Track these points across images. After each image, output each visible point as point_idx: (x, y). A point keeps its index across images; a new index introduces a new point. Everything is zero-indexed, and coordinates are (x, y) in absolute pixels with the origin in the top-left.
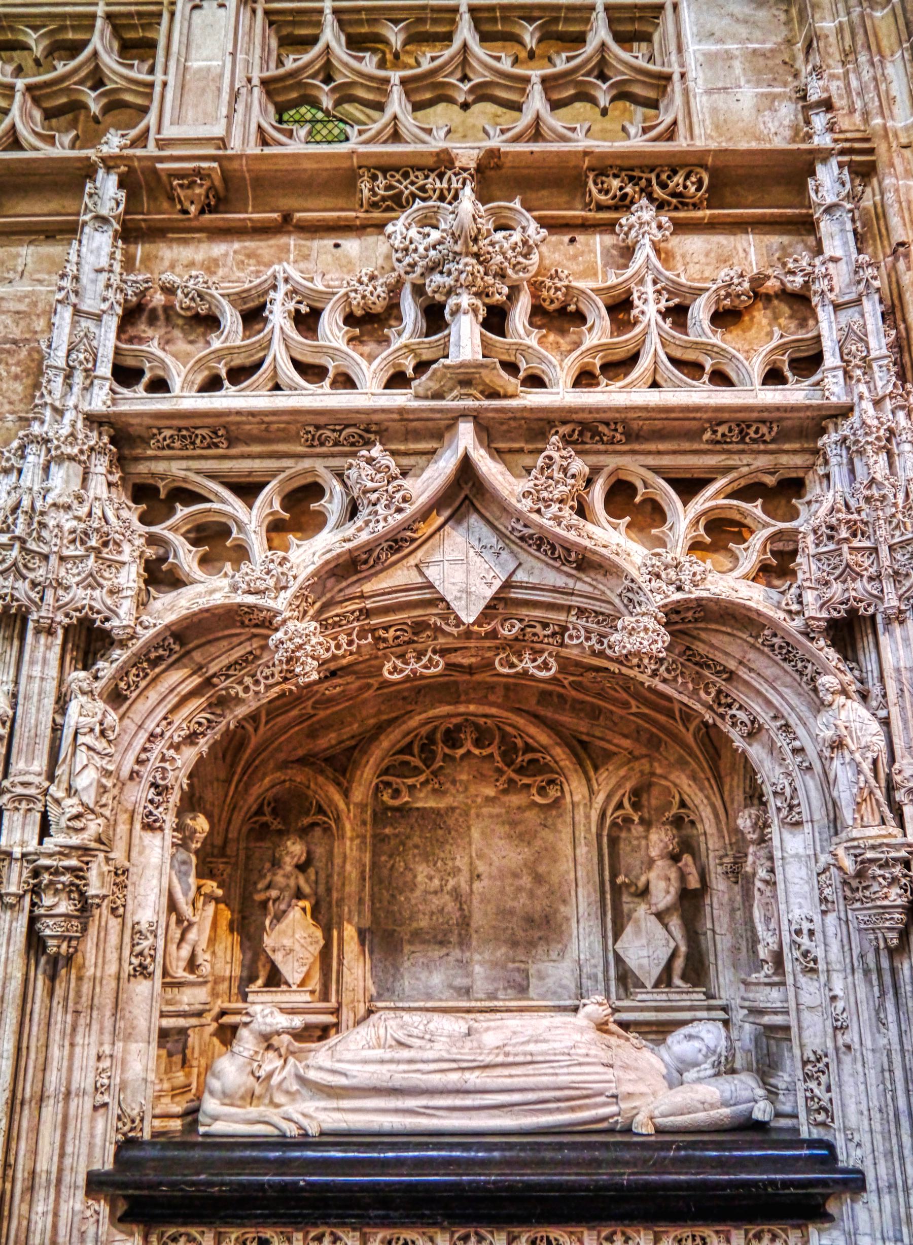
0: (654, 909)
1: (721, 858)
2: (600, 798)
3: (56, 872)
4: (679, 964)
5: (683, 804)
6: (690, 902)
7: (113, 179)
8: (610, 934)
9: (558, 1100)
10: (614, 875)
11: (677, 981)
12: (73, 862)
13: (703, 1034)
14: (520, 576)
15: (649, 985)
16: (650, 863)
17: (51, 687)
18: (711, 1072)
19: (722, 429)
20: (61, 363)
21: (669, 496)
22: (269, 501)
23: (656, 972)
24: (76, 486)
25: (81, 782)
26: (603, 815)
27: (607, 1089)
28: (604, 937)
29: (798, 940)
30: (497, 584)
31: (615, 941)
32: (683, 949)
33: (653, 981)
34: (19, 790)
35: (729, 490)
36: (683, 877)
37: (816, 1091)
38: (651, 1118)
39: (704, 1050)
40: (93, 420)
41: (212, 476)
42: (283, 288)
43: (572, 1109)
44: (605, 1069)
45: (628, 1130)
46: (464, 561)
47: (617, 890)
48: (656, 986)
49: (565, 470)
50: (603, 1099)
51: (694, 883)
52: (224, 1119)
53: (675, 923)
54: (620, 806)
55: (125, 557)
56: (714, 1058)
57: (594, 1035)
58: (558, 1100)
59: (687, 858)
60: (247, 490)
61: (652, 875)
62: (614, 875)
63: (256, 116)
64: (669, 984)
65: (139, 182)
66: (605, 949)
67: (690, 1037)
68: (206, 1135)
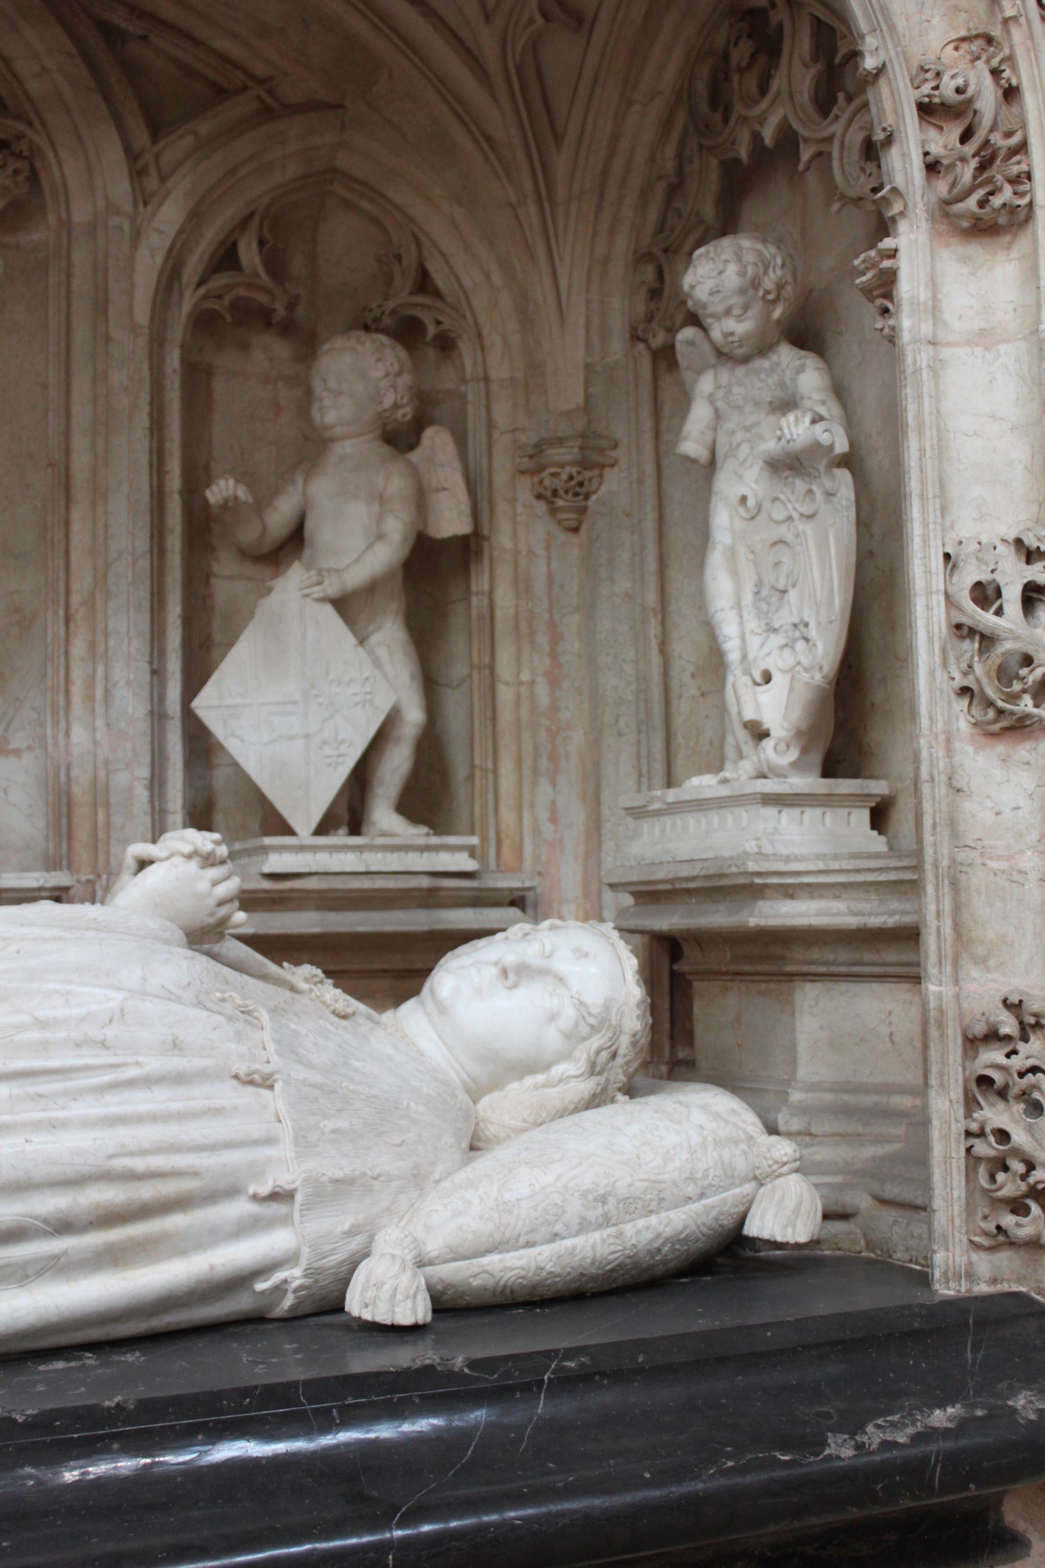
0: (332, 587)
1: (539, 448)
2: (170, 214)
4: (396, 766)
5: (424, 283)
6: (432, 581)
8: (174, 665)
9: (64, 1226)
10: (196, 479)
11: (384, 815)
13: (563, 964)
15: (304, 818)
16: (310, 449)
18: (586, 1087)
23: (329, 782)
26: (171, 275)
27: (256, 1171)
28: (157, 673)
29: (987, 619)
31: (193, 684)
32: (414, 715)
33: (316, 816)
36: (421, 500)
37: (1019, 1137)
38: (421, 1264)
39: (569, 1014)
44: (247, 1096)
45: (325, 1307)
47: (203, 528)
48: (322, 829)
50: (239, 1208)
51: (451, 520)
53: (390, 635)
54: (226, 258)
56: (596, 1042)
57: (186, 967)
58: (64, 1226)
59: (437, 441)
61: (322, 489)
62: (196, 479)
64: (356, 827)
66: (157, 716)
67: (514, 975)
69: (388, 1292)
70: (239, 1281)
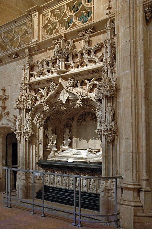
3: (26, 134)
7: (27, 49)
12: (27, 133)
14: (70, 96)
17: (24, 115)
19: (90, 72)
20: (23, 78)
21: (86, 81)
22: (46, 90)
24: (25, 93)
25: (27, 125)
30: (67, 98)
34: (23, 126)
35: (95, 80)
40: (26, 84)
41: (40, 88)
42: (45, 60)
43: (81, 160)
46: (63, 95)
49: (70, 82)
52: (50, 158)
55: (30, 100)
60: (43, 89)
63: (42, 34)
65: (30, 50)
68: (49, 160)
69: (88, 162)
70: (86, 161)
